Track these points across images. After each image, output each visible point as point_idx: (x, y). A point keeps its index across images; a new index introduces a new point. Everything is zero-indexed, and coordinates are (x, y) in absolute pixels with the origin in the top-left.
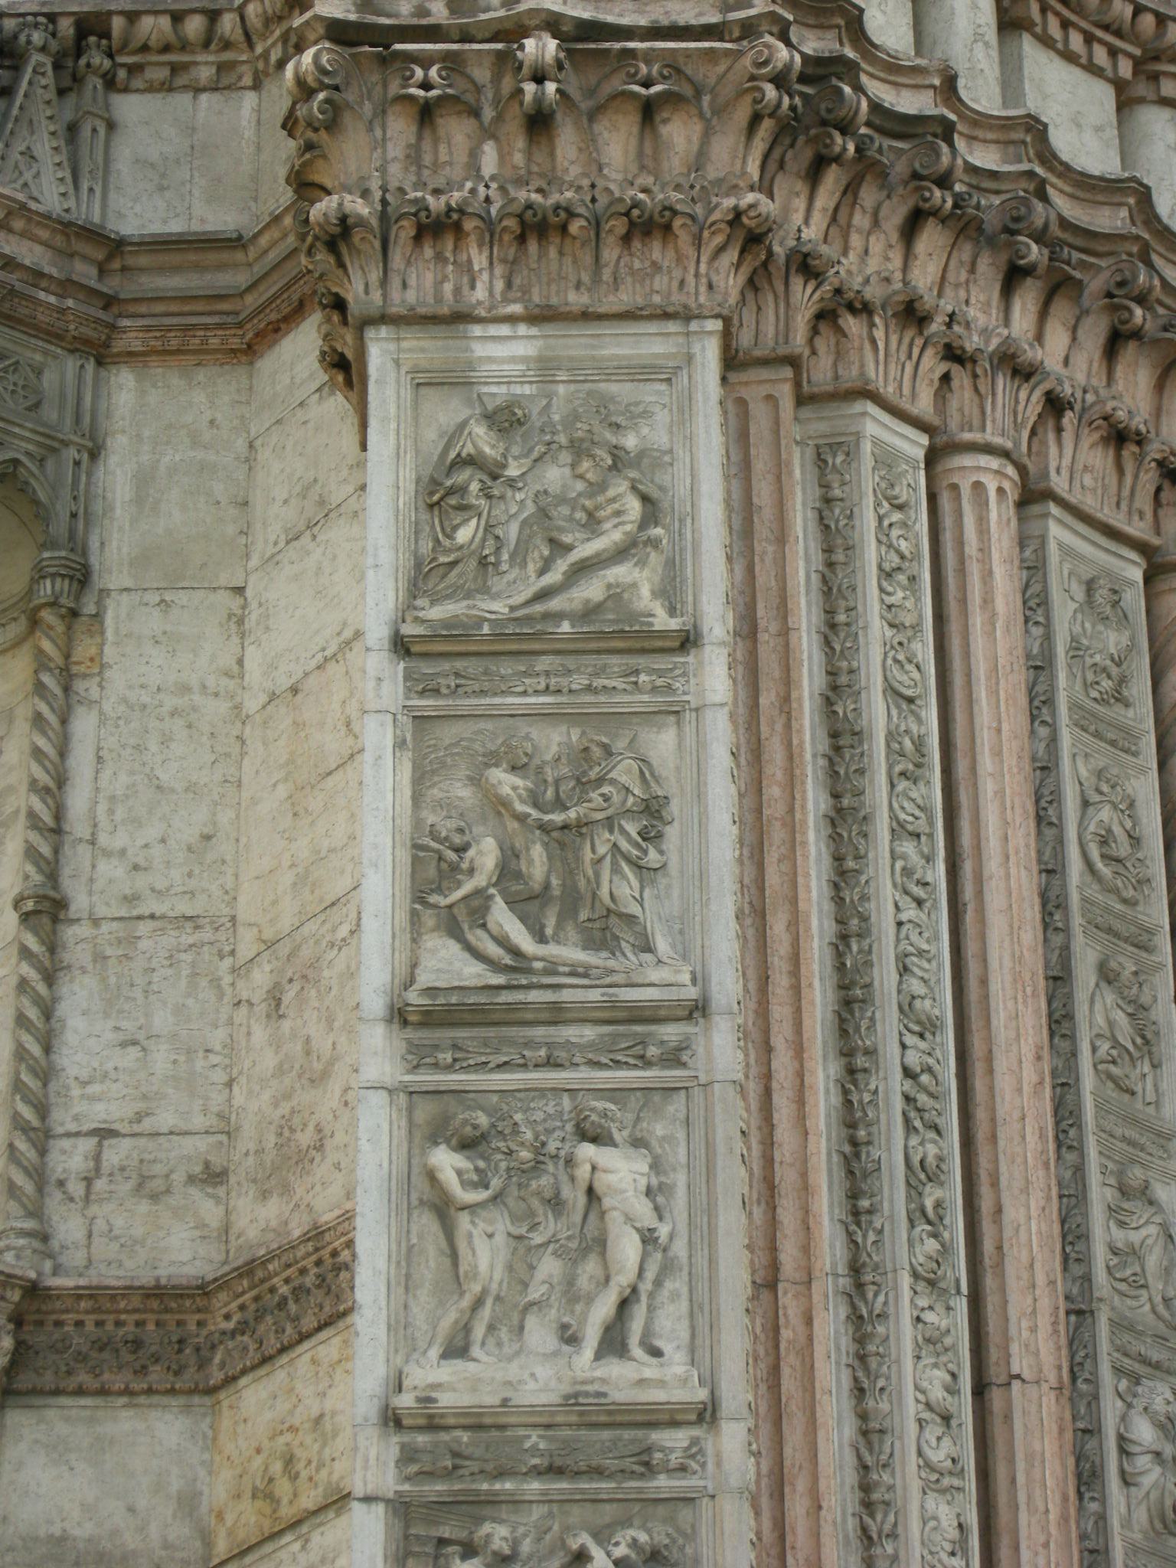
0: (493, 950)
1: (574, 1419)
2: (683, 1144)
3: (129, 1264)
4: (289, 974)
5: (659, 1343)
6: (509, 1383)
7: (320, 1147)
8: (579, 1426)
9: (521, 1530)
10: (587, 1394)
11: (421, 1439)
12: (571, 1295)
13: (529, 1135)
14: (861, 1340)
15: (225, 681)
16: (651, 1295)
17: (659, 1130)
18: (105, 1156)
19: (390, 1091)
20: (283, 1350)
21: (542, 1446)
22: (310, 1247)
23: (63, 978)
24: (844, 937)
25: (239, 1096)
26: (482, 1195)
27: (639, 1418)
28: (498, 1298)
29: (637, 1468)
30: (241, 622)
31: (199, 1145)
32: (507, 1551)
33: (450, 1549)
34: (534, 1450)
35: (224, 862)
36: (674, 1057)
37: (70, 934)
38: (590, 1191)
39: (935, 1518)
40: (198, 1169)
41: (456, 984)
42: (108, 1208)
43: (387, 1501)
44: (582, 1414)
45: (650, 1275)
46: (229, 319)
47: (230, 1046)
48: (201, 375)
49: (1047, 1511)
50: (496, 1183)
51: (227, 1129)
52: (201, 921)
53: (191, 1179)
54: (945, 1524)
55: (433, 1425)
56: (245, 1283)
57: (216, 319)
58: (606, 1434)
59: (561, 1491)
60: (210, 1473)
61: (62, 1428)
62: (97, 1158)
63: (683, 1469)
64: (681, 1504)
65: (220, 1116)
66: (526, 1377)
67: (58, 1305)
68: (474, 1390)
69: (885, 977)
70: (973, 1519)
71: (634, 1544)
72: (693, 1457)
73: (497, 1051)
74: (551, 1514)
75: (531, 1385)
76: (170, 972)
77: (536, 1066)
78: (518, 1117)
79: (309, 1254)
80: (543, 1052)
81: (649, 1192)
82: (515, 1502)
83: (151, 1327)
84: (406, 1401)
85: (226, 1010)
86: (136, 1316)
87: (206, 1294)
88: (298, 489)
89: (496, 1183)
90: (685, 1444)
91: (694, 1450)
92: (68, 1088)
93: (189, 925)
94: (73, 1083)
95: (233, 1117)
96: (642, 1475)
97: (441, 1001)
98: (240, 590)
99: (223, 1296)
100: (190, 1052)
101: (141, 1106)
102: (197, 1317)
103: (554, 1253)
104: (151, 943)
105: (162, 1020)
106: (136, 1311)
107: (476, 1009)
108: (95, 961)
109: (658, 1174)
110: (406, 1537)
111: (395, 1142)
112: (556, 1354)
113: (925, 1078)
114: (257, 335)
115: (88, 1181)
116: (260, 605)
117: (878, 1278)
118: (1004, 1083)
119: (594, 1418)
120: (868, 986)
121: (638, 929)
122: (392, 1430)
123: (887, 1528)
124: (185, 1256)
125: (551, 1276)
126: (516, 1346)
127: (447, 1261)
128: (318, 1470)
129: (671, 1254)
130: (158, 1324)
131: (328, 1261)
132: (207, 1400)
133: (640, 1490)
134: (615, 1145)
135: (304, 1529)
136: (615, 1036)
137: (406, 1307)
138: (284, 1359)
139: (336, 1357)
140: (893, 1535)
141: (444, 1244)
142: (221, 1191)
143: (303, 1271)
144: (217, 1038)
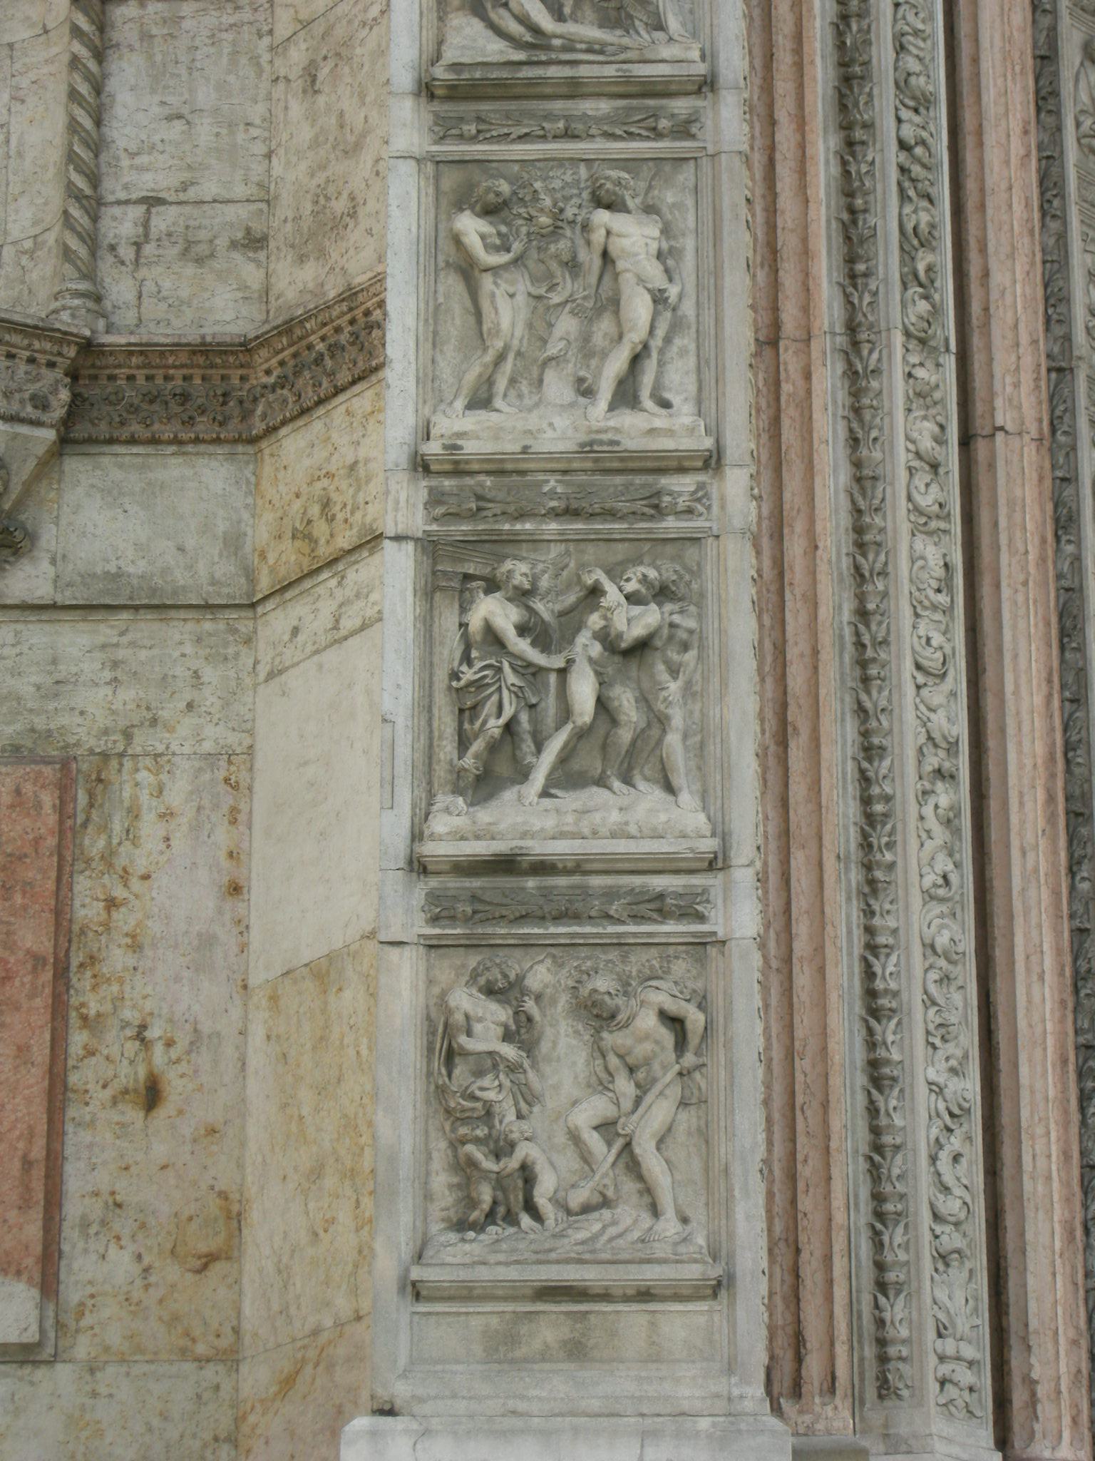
0: (514, 28)
1: (589, 465)
2: (692, 212)
3: (176, 323)
4: (324, 52)
5: (668, 395)
6: (530, 432)
7: (353, 214)
8: (594, 471)
9: (540, 566)
10: (601, 443)
11: (448, 483)
12: (587, 350)
13: (548, 202)
14: (856, 394)
16: (661, 351)
17: (670, 197)
18: (153, 222)
19: (418, 161)
20: (320, 402)
21: (559, 490)
22: (344, 306)
23: (112, 55)
24: (845, 18)
25: (277, 167)
26: (504, 258)
27: (649, 464)
28: (519, 354)
29: (646, 510)
31: (243, 212)
32: (527, 586)
33: (474, 584)
34: (552, 494)
36: (684, 130)
38: (605, 254)
39: (923, 558)
40: (240, 235)
41: (480, 60)
42: (159, 270)
43: (416, 540)
44: (596, 460)
45: (661, 332)
47: (269, 119)
49: (1027, 552)
50: (517, 247)
51: (269, 199)
53: (234, 245)
54: (932, 563)
55: (458, 470)
56: (285, 340)
58: (619, 480)
59: (577, 531)
61: (117, 474)
62: (146, 225)
63: (690, 511)
64: (688, 543)
65: (260, 185)
66: (545, 426)
67: (111, 360)
68: (496, 438)
69: (883, 55)
70: (957, 559)
71: (644, 579)
72: (699, 500)
73: (518, 123)
74: (567, 553)
75: (550, 434)
76: (212, 50)
77: (555, 137)
78: (538, 185)
79: (344, 314)
80: (561, 125)
81: (660, 256)
82: (535, 542)
83: (198, 381)
84: (433, 448)
85: (264, 85)
86: (185, 371)
87: (248, 350)
89: (517, 247)
90: (692, 489)
91: (700, 494)
92: (118, 159)
95: (272, 186)
96: (652, 516)
97: (466, 76)
99: (264, 353)
100: (231, 125)
101: (186, 176)
102: (240, 372)
103: (571, 312)
105: (205, 96)
106: (183, 366)
107: (499, 84)
108: (142, 40)
109: (668, 238)
110: (434, 573)
111: (423, 208)
112: (572, 405)
113: (919, 151)
115: (138, 246)
117: (873, 337)
118: (993, 156)
119: (608, 465)
120: (866, 64)
121: (651, 8)
122: (420, 475)
123: (878, 566)
124: (229, 316)
125: (568, 333)
126: (536, 398)
127: (472, 320)
128: (352, 513)
129: (680, 313)
130: (204, 378)
131: (362, 321)
132: (250, 449)
133: (650, 531)
134: (628, 212)
135: (340, 566)
136: (630, 109)
137: (433, 361)
138: (321, 411)
139: (369, 409)
140: (883, 573)
141: (469, 304)
142: (261, 255)
143: (338, 330)
144: (257, 112)
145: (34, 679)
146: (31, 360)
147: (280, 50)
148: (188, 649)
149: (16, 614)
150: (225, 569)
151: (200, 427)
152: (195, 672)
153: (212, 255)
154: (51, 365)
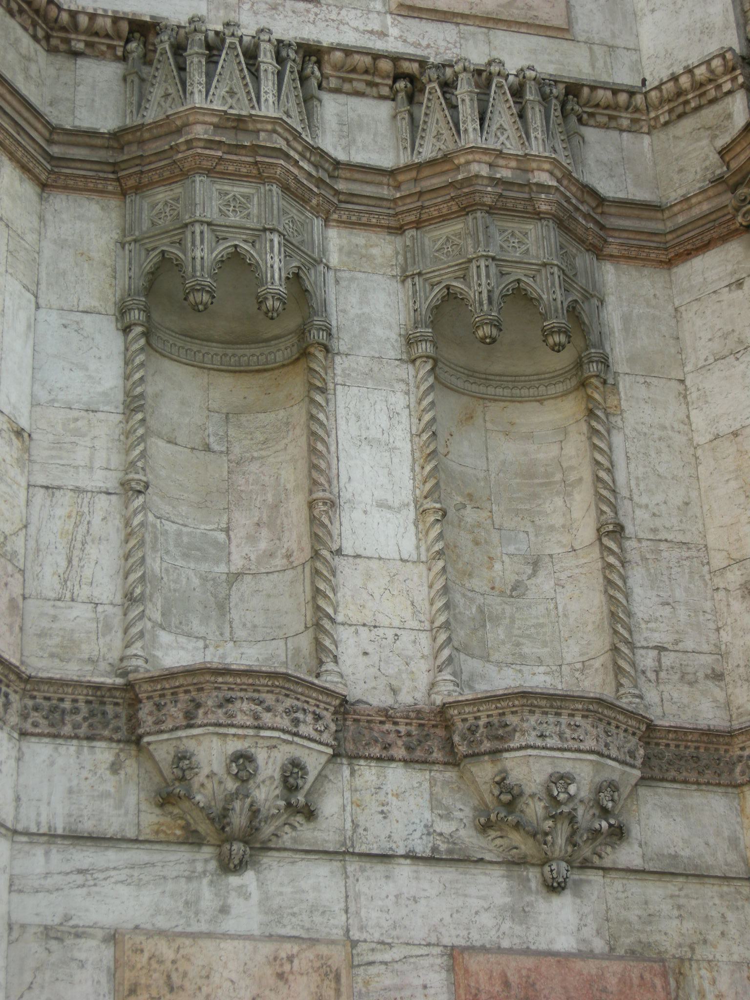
3: (683, 717)
15: (682, 426)
18: (663, 660)
25: (725, 637)
30: (685, 397)
31: (708, 659)
35: (696, 517)
37: (629, 544)
40: (709, 672)
42: (669, 687)
46: (661, 246)
47: (715, 610)
48: (646, 272)
51: (721, 654)
52: (690, 546)
53: (707, 677)
57: (655, 245)
60: (742, 828)
61: (666, 799)
62: (659, 661)
67: (658, 734)
76: (679, 570)
83: (702, 750)
85: (709, 592)
86: (696, 744)
87: (731, 736)
88: (719, 334)
93: (684, 547)
94: (641, 622)
95: (723, 647)
98: (682, 381)
101: (676, 636)
102: (725, 747)
104: (670, 555)
105: (679, 594)
106: (696, 741)
108: (642, 560)
114: (676, 255)
115: (657, 672)
116: (698, 390)
130: (706, 749)
132: (736, 791)
142: (722, 684)
144: (708, 605)
145: (637, 912)
146: (626, 731)
147: (717, 573)
148: (717, 901)
149: (622, 874)
150: (732, 857)
151: (707, 776)
152: (723, 915)
153: (696, 681)
154: (634, 734)
